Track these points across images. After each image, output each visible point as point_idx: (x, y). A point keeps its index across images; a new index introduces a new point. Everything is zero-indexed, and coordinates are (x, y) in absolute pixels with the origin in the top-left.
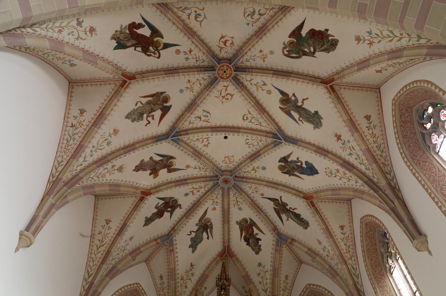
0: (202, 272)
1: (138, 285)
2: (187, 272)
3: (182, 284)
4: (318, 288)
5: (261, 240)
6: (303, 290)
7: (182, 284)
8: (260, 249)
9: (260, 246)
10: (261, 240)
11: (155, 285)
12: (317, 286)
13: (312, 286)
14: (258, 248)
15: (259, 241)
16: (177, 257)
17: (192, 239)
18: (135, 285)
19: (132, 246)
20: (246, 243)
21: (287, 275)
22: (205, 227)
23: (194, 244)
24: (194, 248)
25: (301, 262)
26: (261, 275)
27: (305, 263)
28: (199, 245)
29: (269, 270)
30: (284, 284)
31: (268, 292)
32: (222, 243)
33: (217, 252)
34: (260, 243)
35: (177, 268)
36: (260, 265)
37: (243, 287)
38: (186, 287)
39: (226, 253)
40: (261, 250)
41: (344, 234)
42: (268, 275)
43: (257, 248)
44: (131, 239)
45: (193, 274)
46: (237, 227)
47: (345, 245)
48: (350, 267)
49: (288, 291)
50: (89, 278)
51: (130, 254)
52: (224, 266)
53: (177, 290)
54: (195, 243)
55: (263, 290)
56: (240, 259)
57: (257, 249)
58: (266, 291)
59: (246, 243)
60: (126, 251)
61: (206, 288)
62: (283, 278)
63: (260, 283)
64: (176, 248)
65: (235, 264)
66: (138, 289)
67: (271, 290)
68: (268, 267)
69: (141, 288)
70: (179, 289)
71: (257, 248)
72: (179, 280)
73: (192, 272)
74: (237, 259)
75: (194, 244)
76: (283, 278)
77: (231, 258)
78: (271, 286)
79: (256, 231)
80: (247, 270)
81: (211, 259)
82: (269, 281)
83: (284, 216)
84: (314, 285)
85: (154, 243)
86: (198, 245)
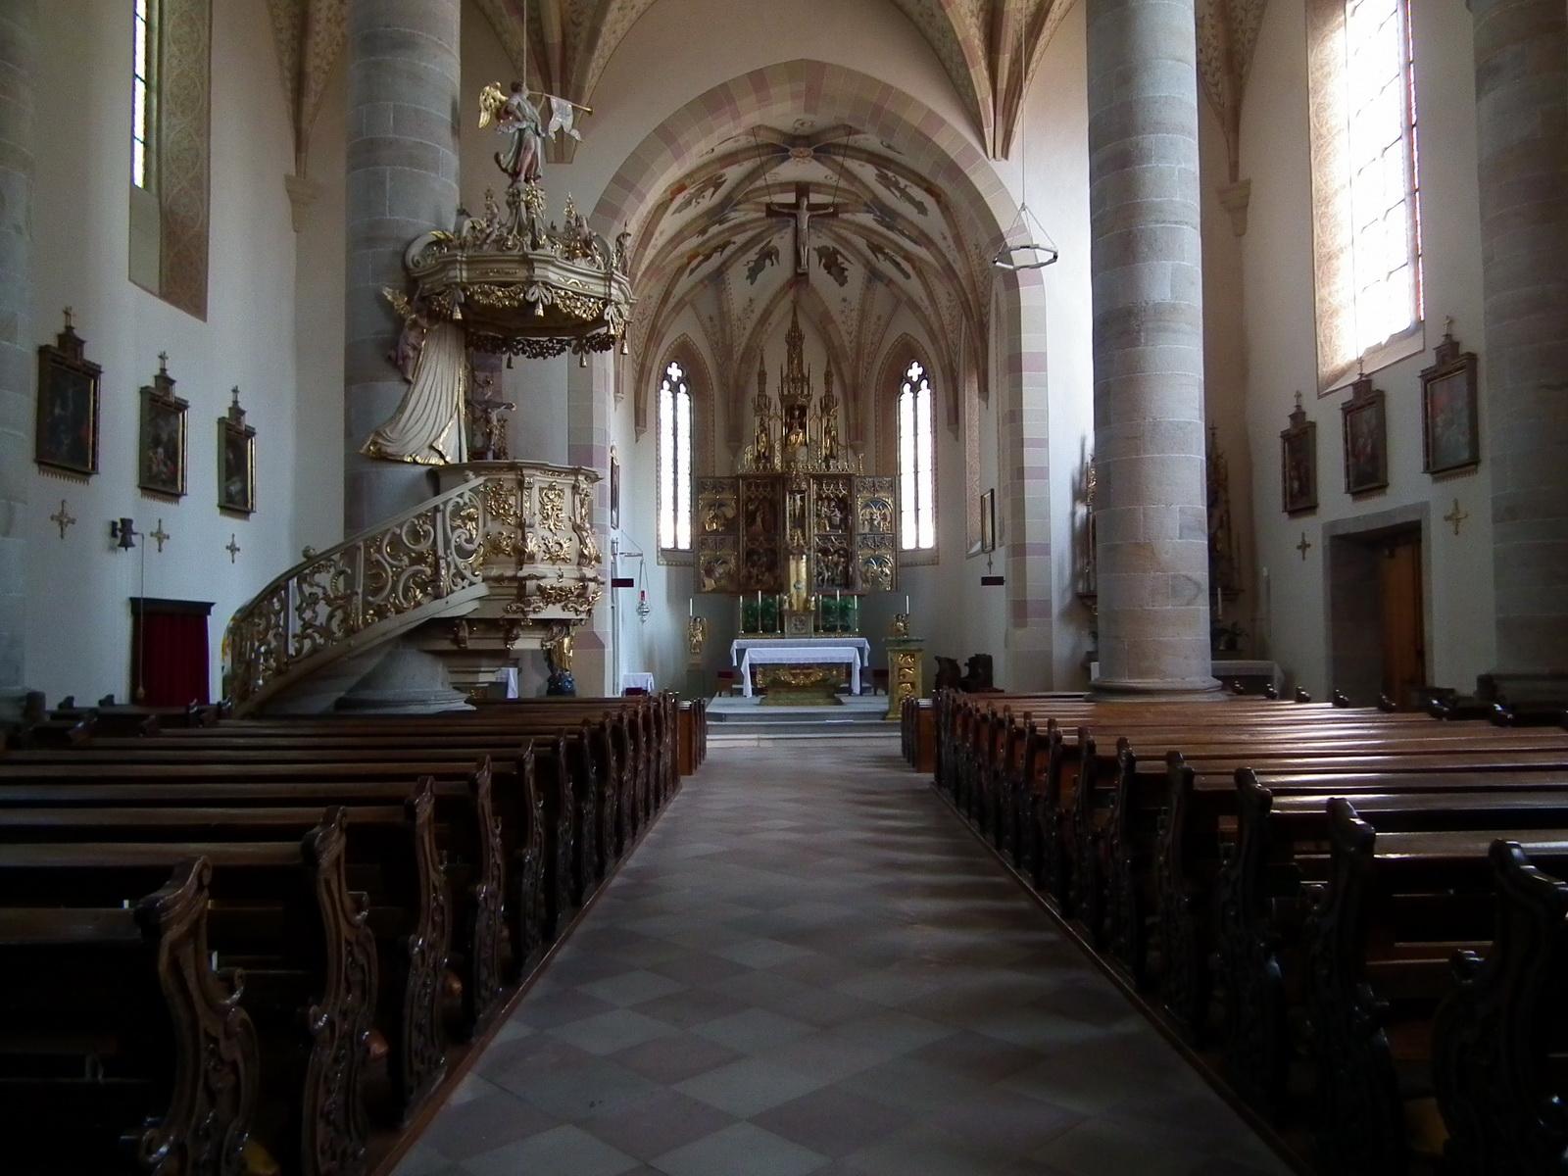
2: (745, 309)
5: (847, 270)
9: (846, 277)
17: (749, 269)
22: (769, 254)
34: (846, 273)
38: (744, 329)
39: (799, 278)
41: (950, 301)
42: (854, 314)
45: (752, 311)
46: (815, 253)
47: (950, 314)
48: (950, 342)
50: (638, 357)
54: (753, 273)
68: (856, 304)
79: (840, 259)
83: (879, 256)
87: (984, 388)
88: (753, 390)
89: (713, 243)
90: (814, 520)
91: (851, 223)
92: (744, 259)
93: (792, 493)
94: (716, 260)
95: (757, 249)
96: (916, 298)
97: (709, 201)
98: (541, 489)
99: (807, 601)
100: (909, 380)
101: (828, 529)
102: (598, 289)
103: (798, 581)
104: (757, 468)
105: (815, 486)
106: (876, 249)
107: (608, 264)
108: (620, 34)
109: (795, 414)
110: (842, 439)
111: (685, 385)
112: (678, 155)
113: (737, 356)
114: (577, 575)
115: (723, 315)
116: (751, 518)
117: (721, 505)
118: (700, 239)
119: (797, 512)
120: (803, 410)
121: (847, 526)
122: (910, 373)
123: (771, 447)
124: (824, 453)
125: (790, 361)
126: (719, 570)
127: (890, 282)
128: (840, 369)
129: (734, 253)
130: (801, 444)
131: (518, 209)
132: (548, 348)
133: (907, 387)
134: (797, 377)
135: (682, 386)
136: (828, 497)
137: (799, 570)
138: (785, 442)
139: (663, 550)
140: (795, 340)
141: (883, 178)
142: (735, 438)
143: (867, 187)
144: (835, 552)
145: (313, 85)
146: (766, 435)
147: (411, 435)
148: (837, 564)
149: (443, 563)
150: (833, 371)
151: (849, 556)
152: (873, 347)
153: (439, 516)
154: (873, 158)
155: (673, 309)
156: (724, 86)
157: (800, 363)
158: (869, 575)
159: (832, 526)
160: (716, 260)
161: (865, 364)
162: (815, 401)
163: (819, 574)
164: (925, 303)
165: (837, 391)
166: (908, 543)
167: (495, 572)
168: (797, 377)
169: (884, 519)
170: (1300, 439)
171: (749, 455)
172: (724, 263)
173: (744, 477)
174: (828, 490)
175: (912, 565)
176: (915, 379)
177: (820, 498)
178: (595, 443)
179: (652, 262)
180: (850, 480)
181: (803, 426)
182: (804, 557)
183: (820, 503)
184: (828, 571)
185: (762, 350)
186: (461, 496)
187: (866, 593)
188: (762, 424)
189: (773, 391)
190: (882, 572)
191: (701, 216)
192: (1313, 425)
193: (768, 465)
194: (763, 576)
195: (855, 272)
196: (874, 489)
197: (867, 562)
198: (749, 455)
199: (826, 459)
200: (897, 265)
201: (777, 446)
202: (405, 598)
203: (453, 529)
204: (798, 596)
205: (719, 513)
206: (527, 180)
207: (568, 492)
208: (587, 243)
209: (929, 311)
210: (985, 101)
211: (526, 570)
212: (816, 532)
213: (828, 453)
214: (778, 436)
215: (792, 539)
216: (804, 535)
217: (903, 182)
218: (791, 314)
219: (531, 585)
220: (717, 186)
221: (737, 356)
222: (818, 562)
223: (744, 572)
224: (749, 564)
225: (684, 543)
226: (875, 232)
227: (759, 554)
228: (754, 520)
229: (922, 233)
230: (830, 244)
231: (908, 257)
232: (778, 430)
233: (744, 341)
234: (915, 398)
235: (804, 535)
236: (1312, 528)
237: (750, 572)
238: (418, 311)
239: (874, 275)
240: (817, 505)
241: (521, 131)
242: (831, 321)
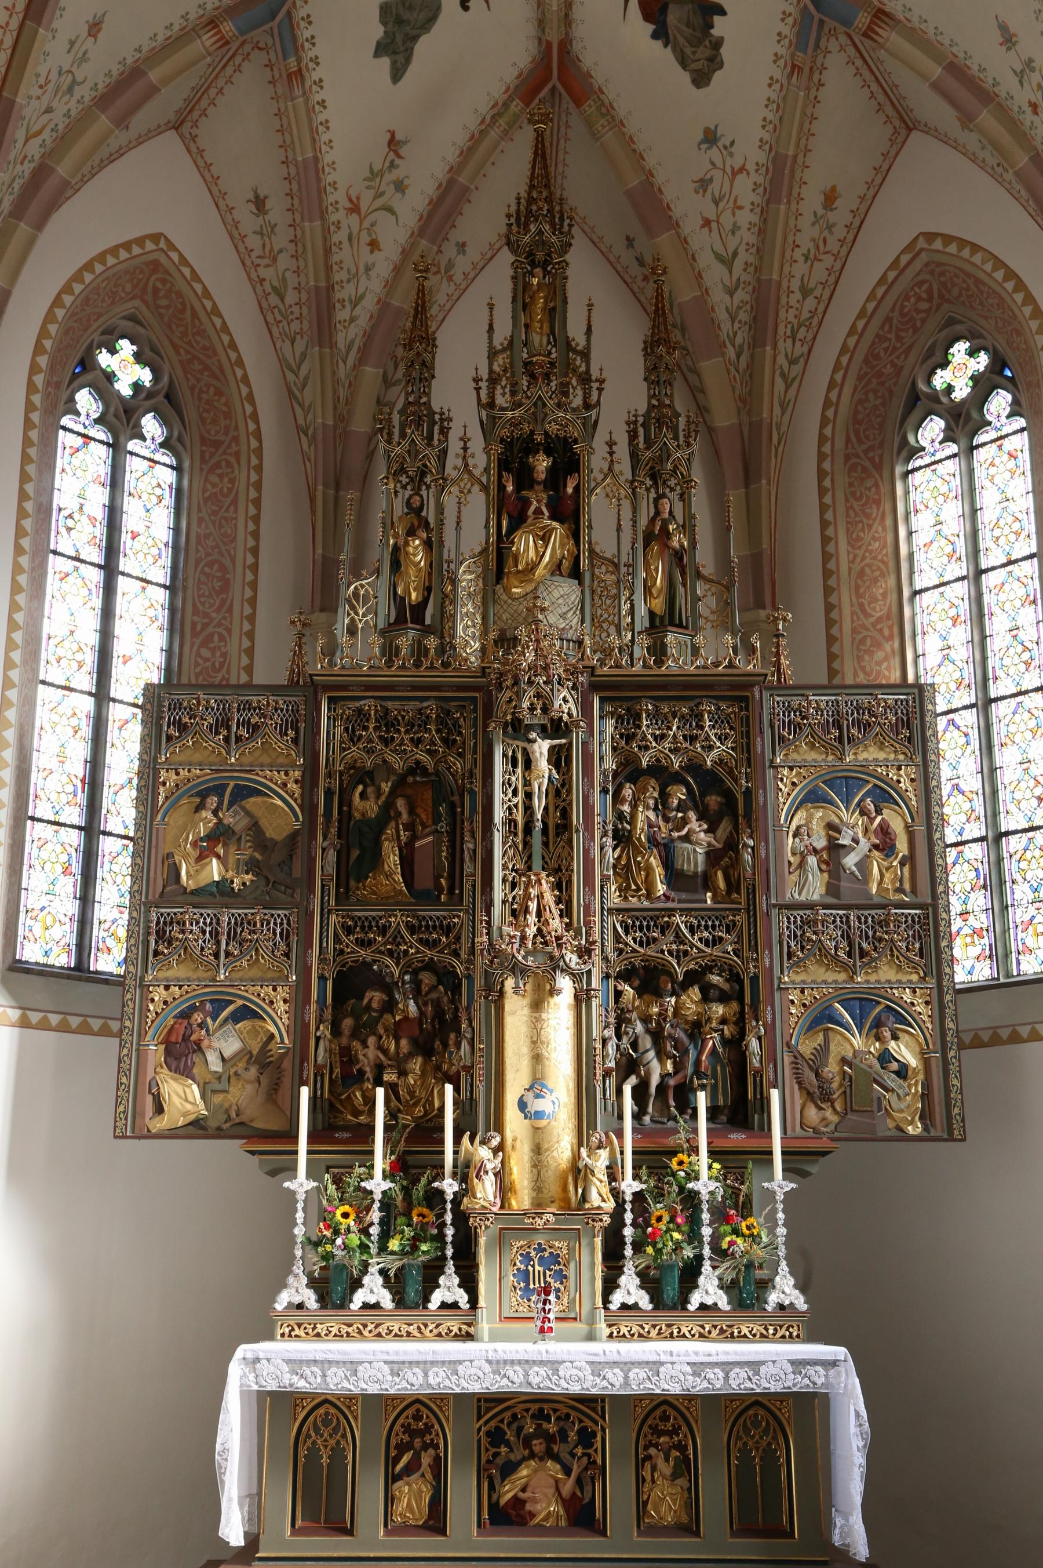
0: (440, 172)
1: (162, 244)
2: (374, 175)
3: (355, 231)
4: (966, 253)
5: (722, 12)
6: (897, 259)
7: (355, 231)
8: (715, 62)
9: (718, 44)
10: (722, 12)
11: (237, 238)
12: (962, 243)
13: (938, 245)
14: (709, 53)
15: (717, 19)
16: (322, 103)
18: (150, 246)
19: (102, 64)
20: (650, 28)
21: (834, 189)
23: (399, 38)
24: (401, 58)
25: (906, 123)
26: (715, 188)
27: (927, 130)
28: (424, 39)
29: (751, 167)
30: (815, 232)
31: (738, 265)
32: (531, 29)
33: (510, 76)
35: (327, 159)
36: (710, 138)
37: (630, 241)
38: (374, 245)
39: (554, 81)
40: (721, 66)
42: (745, 190)
43: (703, 52)
44: (95, 28)
45: (400, 186)
49: (828, 260)
51: (104, 101)
52: (541, 154)
53: (336, 258)
55: (719, 257)
56: (621, 110)
57: (702, 61)
58: (728, 262)
59: (650, 28)
60: (84, 92)
61: (462, 247)
62: (812, 200)
63: (707, 223)
64: (316, 60)
65: (595, 136)
66: (163, 259)
67: (751, 259)
68: (750, 151)
69: (175, 256)
70: (343, 255)
71: (703, 52)
72: (341, 215)
73: (396, 174)
74: (607, 110)
75: (399, 38)
76: (812, 200)
77: (578, 103)
78: (753, 239)
80: (650, 161)
81: (484, 107)
82: (746, 217)
84: (948, 239)
85: (208, 39)
86: (415, 38)
93: (517, 729)
99: (578, 1172)
100: (938, 403)
101: (661, 889)
103: (537, 1085)
104: (390, 652)
105: (610, 725)
110: (705, 557)
111: (164, 420)
117: (242, 793)
119: (539, 805)
120: (567, 460)
121: (733, 879)
124: (642, 611)
125: (522, 299)
126: (225, 1044)
130: (556, 569)
133: (934, 428)
134: (543, 360)
135: (150, 425)
136: (660, 772)
138: (499, 563)
144: (692, 978)
146: (428, 544)
148: (696, 1029)
151: (743, 994)
152: (810, 303)
157: (556, 313)
158: (832, 1069)
159: (674, 877)
161: (781, 360)
163: (629, 1066)
165: (681, 403)
168: (543, 360)
169: (885, 844)
173: (338, 691)
174: (661, 743)
175: (996, 1040)
177: (629, 771)
180: (744, 701)
181: (569, 513)
182: (565, 983)
183: (628, 792)
184: (661, 1055)
187: (823, 1144)
188: (415, 511)
189: (456, 389)
190: (885, 1057)
193: (432, 642)
194: (403, 1073)
196: (840, 732)
197: (822, 1019)
199: (657, 625)
201: (467, 579)
204: (538, 1150)
212: (614, 899)
213: (658, 605)
215: (518, 914)
221: (352, 327)
222: (621, 1021)
224: (348, 1023)
227: (388, 988)
233: (373, 286)
235: (565, 901)
240: (617, 798)
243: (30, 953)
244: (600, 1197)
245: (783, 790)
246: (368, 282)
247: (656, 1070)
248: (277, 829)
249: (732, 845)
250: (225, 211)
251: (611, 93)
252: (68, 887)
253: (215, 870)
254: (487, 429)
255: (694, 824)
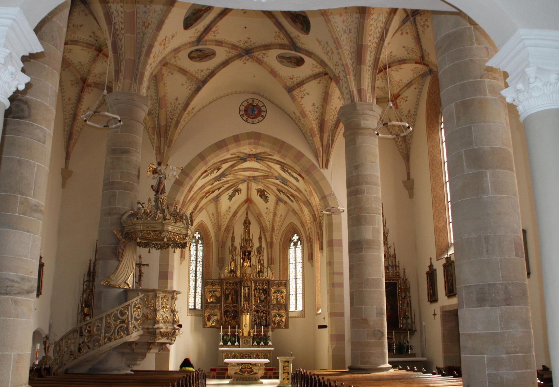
0: (235, 210)
22: (238, 191)
36: (267, 208)
39: (248, 201)
42: (271, 214)
54: (231, 198)
58: (269, 222)
70: (223, 220)
74: (255, 204)
79: (266, 193)
82: (271, 217)
87: (321, 248)
88: (229, 243)
89: (215, 188)
90: (253, 298)
91: (270, 182)
92: (227, 193)
93: (244, 287)
94: (217, 192)
95: (233, 189)
96: (296, 210)
97: (215, 174)
98: (162, 298)
102: (184, 232)
106: (279, 191)
107: (187, 223)
108: (186, 121)
109: (246, 254)
110: (265, 264)
112: (206, 164)
113: (223, 228)
114: (172, 327)
115: (218, 213)
116: (227, 297)
117: (214, 291)
118: (211, 186)
120: (250, 253)
122: (294, 238)
123: (236, 267)
125: (245, 232)
127: (285, 203)
128: (265, 235)
129: (223, 191)
131: (158, 203)
132: (163, 246)
133: (292, 244)
136: (259, 289)
137: (246, 319)
138: (242, 266)
139: (190, 309)
140: (247, 224)
141: (283, 169)
142: (221, 263)
143: (276, 171)
145: (74, 136)
147: (119, 278)
148: (262, 317)
149: (130, 323)
150: (263, 236)
151: (268, 313)
153: (130, 307)
154: (278, 162)
155: (198, 211)
156: (224, 140)
158: (276, 321)
159: (260, 300)
160: (217, 192)
162: (255, 249)
163: (255, 321)
164: (299, 212)
165: (264, 245)
166: (292, 308)
167: (146, 326)
168: (247, 240)
169: (282, 298)
170: (431, 274)
171: (226, 271)
172: (219, 194)
174: (259, 287)
176: (296, 240)
177: (256, 289)
178: (169, 270)
179: (192, 197)
181: (249, 259)
185: (233, 228)
186: (137, 300)
191: (212, 180)
192: (435, 270)
195: (272, 199)
197: (275, 316)
198: (226, 271)
199: (259, 273)
200: (289, 197)
201: (239, 267)
202: (118, 335)
203: (134, 311)
205: (214, 295)
206: (161, 194)
207: (170, 299)
208: (182, 218)
209: (301, 215)
210: (319, 148)
211: (156, 326)
214: (239, 263)
216: (249, 304)
217: (290, 171)
218: (245, 214)
219: (158, 331)
220: (219, 169)
221: (223, 228)
222: (254, 316)
223: (223, 319)
225: (198, 307)
226: (279, 185)
227: (230, 312)
228: (228, 298)
229: (297, 188)
230: (262, 188)
231: (293, 195)
232: (239, 259)
233: (226, 223)
234: (296, 248)
235: (249, 304)
236: (436, 307)
237: (226, 320)
238: (125, 238)
239: (279, 200)
241: (160, 178)
242: (262, 216)
243: (190, 307)
244: (252, 334)
245: (272, 291)
246: (225, 223)
247: (258, 321)
248: (218, 295)
249: (266, 297)
250: (209, 215)
251: (256, 202)
252: (193, 299)
253: (212, 300)
254: (241, 249)
255: (263, 295)
